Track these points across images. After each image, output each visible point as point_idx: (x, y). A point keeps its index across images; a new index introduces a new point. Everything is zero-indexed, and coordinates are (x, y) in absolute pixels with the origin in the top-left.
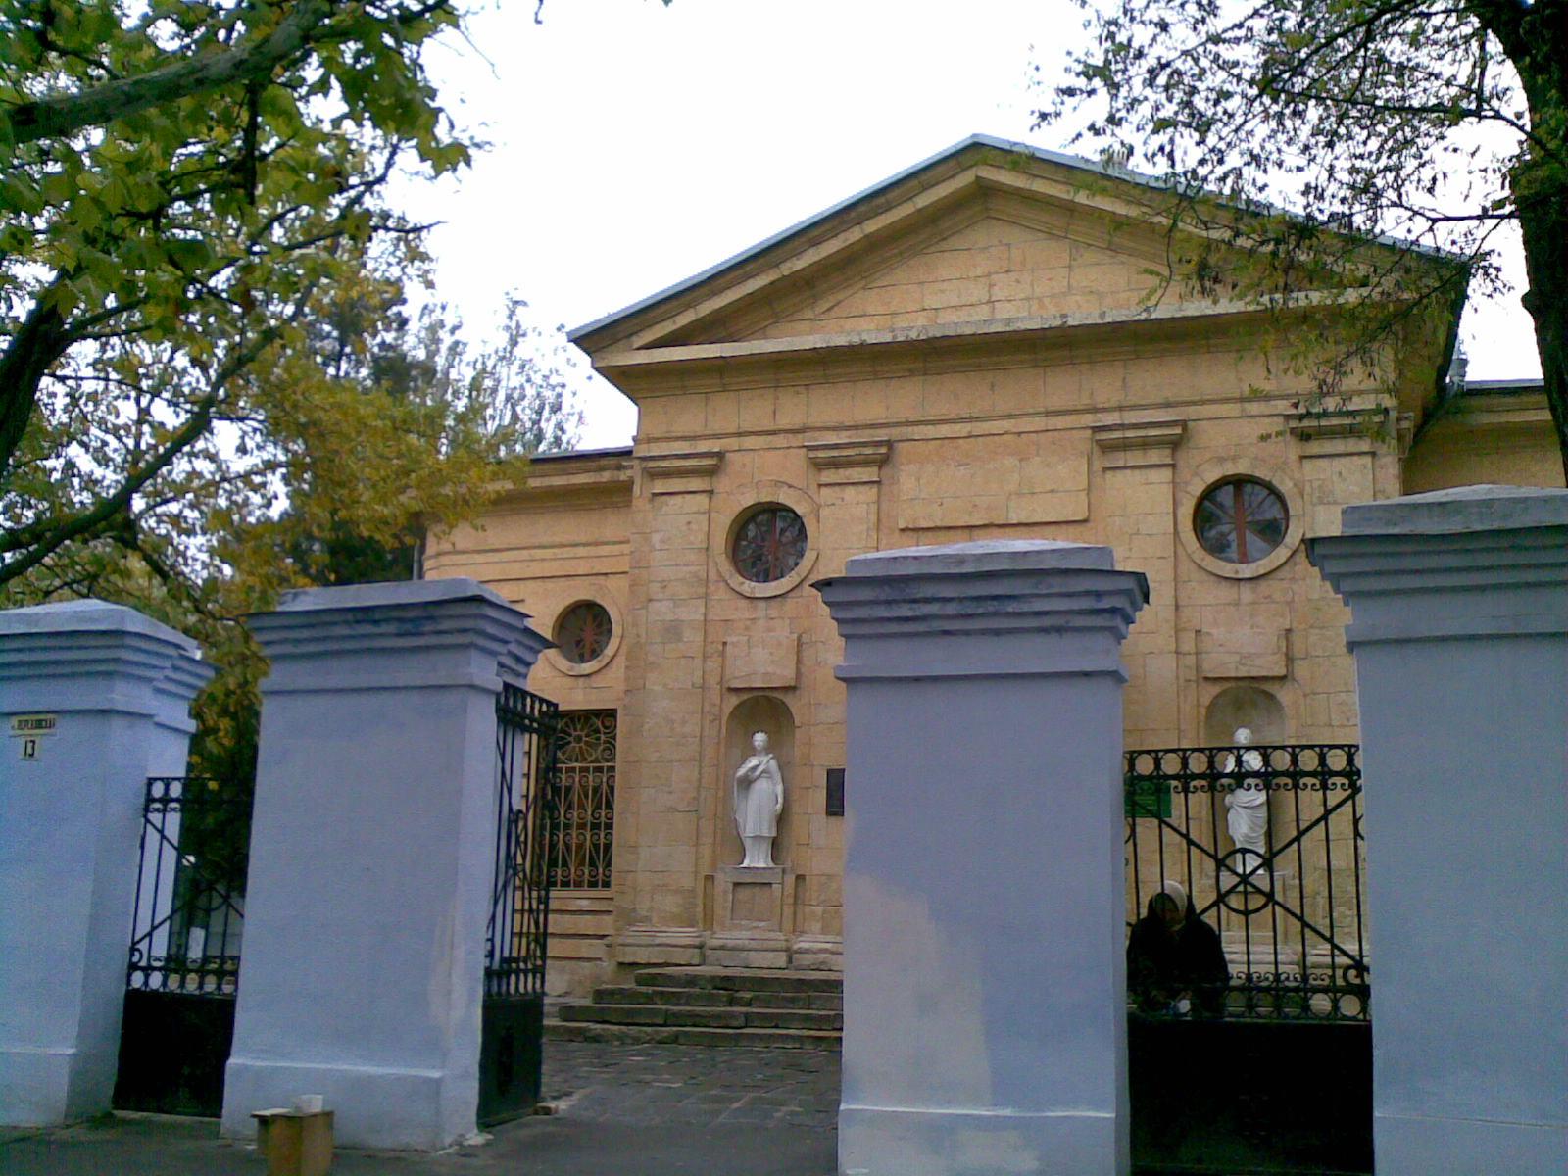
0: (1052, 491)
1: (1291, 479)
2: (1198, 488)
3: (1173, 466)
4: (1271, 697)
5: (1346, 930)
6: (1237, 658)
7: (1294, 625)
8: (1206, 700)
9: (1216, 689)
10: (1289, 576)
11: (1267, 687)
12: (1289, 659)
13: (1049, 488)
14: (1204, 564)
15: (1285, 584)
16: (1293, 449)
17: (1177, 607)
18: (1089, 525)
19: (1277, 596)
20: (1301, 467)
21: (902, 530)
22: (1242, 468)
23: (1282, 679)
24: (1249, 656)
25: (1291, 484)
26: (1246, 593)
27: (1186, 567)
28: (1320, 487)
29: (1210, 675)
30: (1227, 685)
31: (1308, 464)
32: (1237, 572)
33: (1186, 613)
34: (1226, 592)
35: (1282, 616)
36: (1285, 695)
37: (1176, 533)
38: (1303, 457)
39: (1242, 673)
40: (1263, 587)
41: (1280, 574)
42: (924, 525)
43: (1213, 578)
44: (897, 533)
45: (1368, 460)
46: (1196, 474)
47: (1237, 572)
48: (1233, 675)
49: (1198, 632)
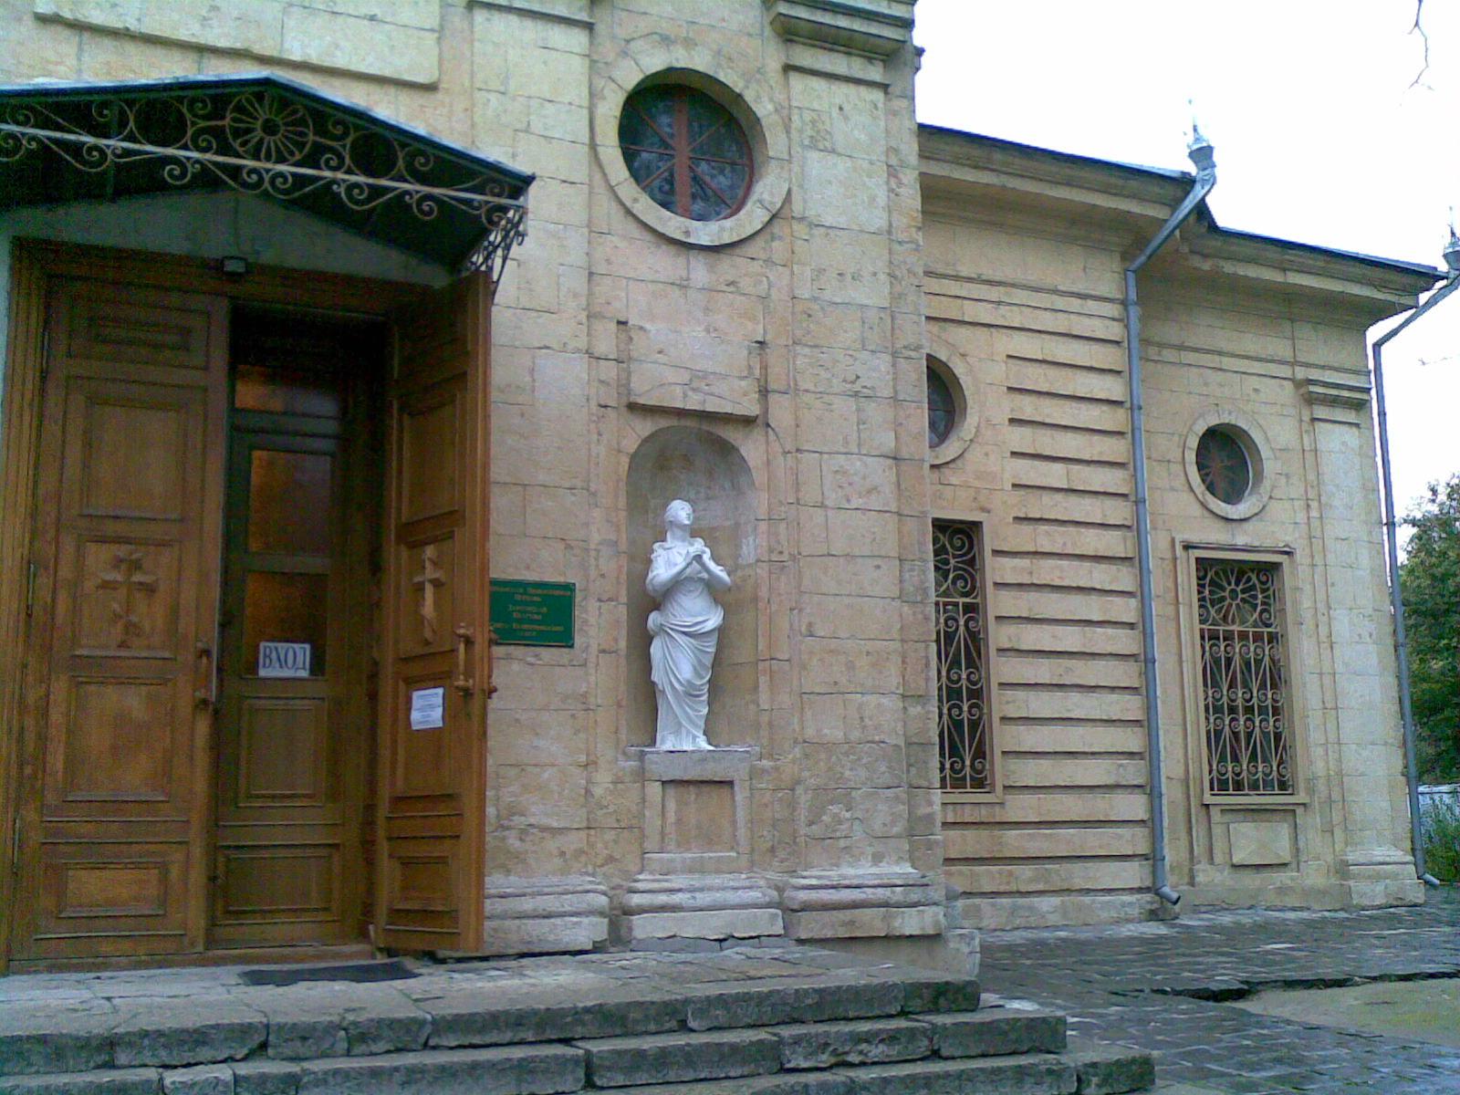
0: (372, 18)
1: (771, 100)
2: (630, 77)
3: (589, 27)
4: (726, 450)
5: (842, 843)
6: (686, 377)
7: (768, 338)
8: (631, 444)
9: (645, 427)
10: (763, 256)
11: (731, 434)
12: (764, 392)
13: (363, 11)
14: (637, 209)
15: (755, 267)
16: (774, 57)
17: (591, 274)
18: (440, 96)
19: (746, 284)
20: (787, 84)
21: (43, 20)
22: (699, 61)
23: (747, 421)
24: (704, 375)
25: (770, 107)
26: (700, 271)
27: (605, 206)
28: (813, 122)
29: (642, 401)
30: (663, 423)
31: (797, 81)
32: (687, 233)
33: (603, 288)
34: (665, 264)
35: (753, 319)
36: (752, 448)
37: (593, 146)
38: (788, 68)
39: (693, 403)
40: (728, 267)
41: (753, 249)
42: (97, 17)
43: (648, 237)
44: (29, 22)
45: (878, 96)
46: (624, 54)
47: (687, 233)
48: (679, 405)
49: (621, 323)
